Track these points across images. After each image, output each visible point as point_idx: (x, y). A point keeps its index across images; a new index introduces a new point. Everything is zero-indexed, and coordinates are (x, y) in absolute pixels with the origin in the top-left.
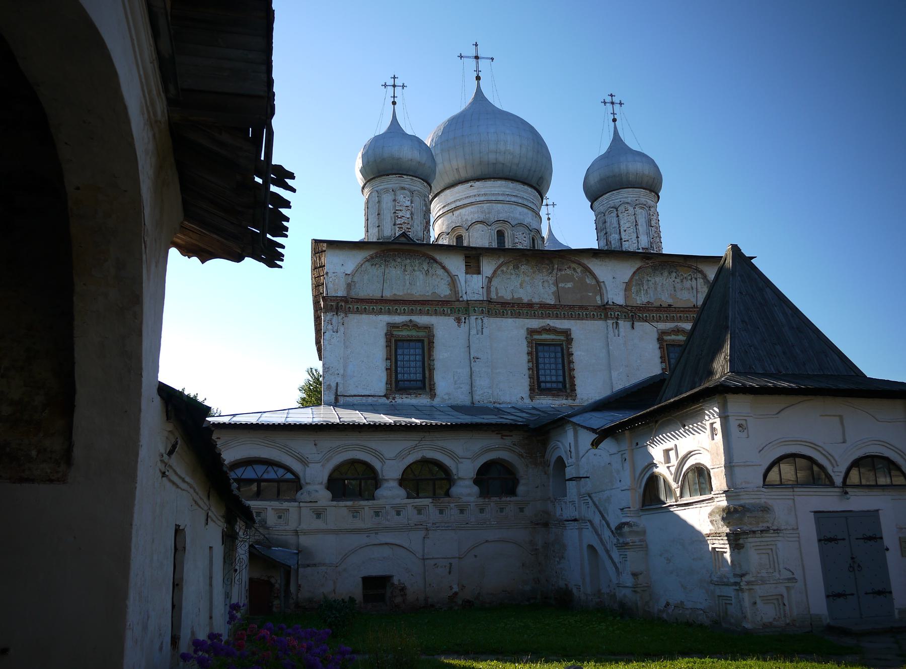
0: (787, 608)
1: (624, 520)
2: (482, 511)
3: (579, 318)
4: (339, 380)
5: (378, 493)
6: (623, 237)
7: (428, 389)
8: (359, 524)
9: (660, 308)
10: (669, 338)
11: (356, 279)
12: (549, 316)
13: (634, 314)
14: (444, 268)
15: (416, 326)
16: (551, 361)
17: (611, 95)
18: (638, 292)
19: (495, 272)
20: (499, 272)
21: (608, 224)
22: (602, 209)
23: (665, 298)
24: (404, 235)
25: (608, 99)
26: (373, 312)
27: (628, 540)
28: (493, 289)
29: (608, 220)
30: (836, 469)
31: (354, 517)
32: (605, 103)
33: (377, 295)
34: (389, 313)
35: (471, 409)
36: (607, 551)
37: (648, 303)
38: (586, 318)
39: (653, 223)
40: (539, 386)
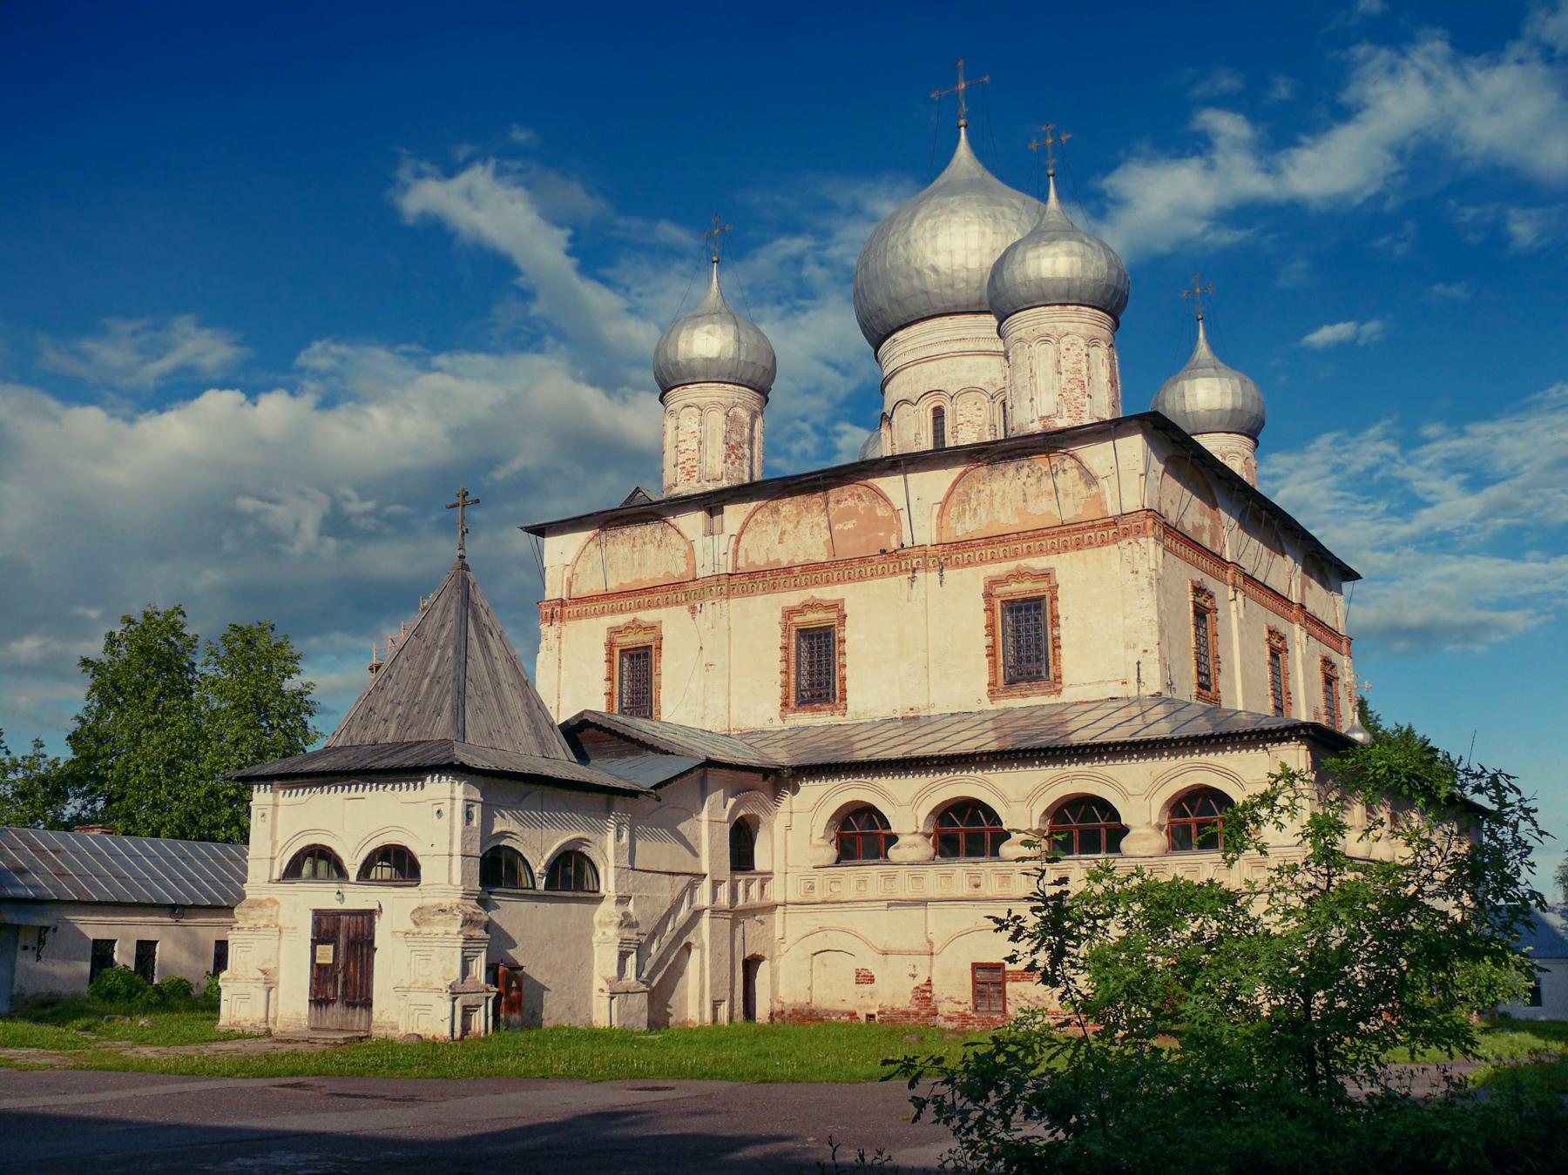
9: (989, 540)
10: (1007, 589)
15: (636, 626)
20: (752, 523)
23: (1007, 519)
28: (741, 553)
33: (600, 589)
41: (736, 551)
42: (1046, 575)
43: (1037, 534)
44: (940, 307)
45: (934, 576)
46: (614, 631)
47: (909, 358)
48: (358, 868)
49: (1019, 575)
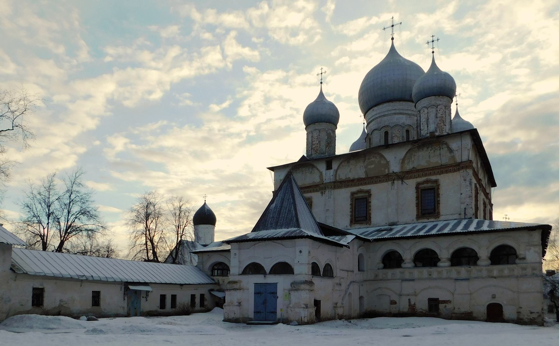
3: (376, 183)
9: (418, 171)
12: (361, 184)
13: (402, 176)
14: (317, 169)
19: (339, 167)
28: (338, 175)
37: (413, 167)
38: (380, 182)
41: (336, 175)
42: (436, 181)
43: (434, 168)
45: (400, 182)
49: (427, 182)
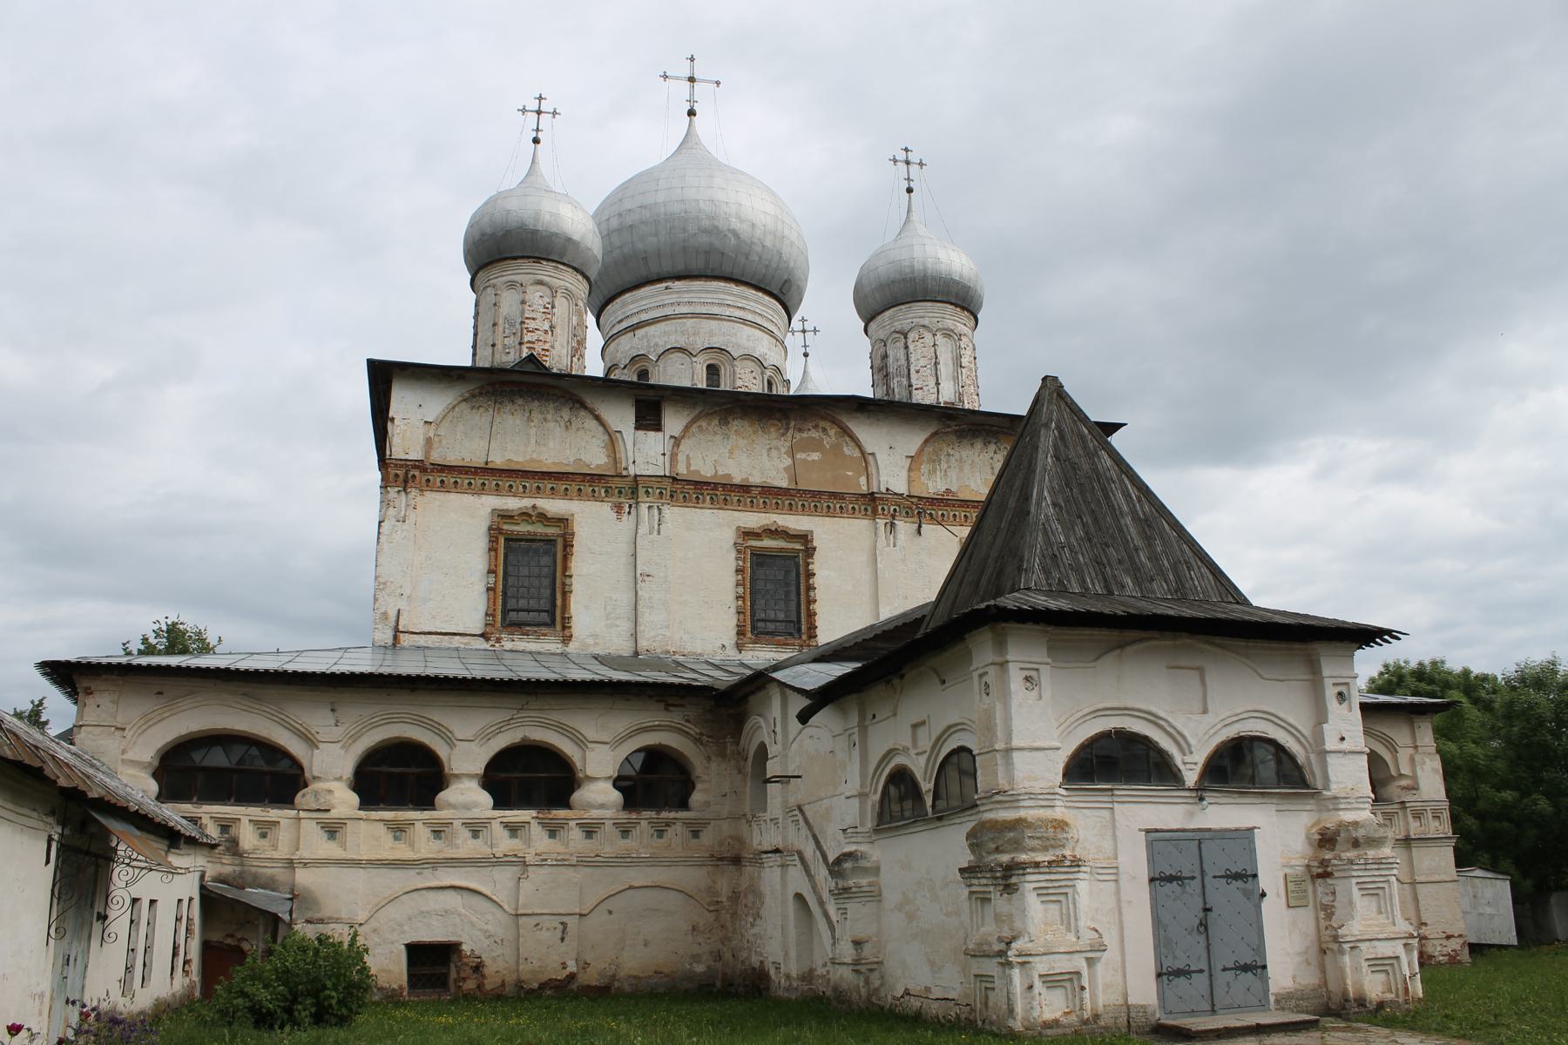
0: (1087, 994)
1: (848, 849)
2: (625, 833)
3: (829, 513)
4: (402, 604)
5: (443, 796)
6: (913, 381)
7: (559, 627)
8: (403, 852)
11: (442, 432)
13: (924, 509)
14: (597, 418)
15: (543, 517)
16: (776, 584)
17: (906, 150)
18: (932, 472)
19: (687, 428)
20: (694, 429)
21: (891, 360)
22: (882, 334)
24: (531, 358)
25: (901, 156)
26: (470, 489)
27: (851, 883)
28: (681, 458)
29: (891, 353)
30: (1187, 759)
31: (396, 838)
32: (895, 161)
33: (477, 460)
34: (498, 490)
35: (635, 658)
36: (821, 903)
37: (948, 491)
39: (965, 361)
40: (753, 628)
41: (674, 457)
44: (727, 270)
46: (505, 516)
47: (684, 309)
48: (1199, 768)
